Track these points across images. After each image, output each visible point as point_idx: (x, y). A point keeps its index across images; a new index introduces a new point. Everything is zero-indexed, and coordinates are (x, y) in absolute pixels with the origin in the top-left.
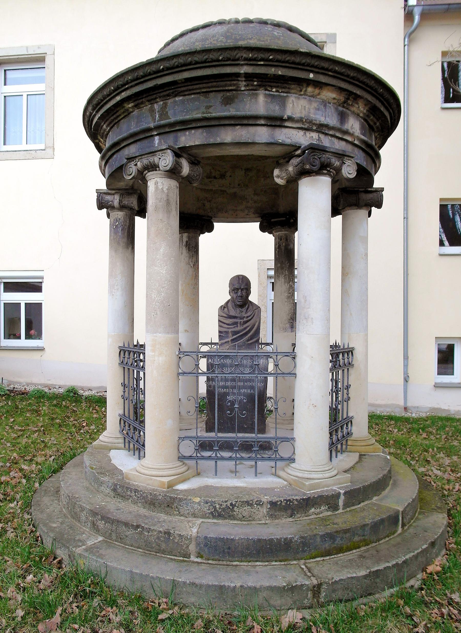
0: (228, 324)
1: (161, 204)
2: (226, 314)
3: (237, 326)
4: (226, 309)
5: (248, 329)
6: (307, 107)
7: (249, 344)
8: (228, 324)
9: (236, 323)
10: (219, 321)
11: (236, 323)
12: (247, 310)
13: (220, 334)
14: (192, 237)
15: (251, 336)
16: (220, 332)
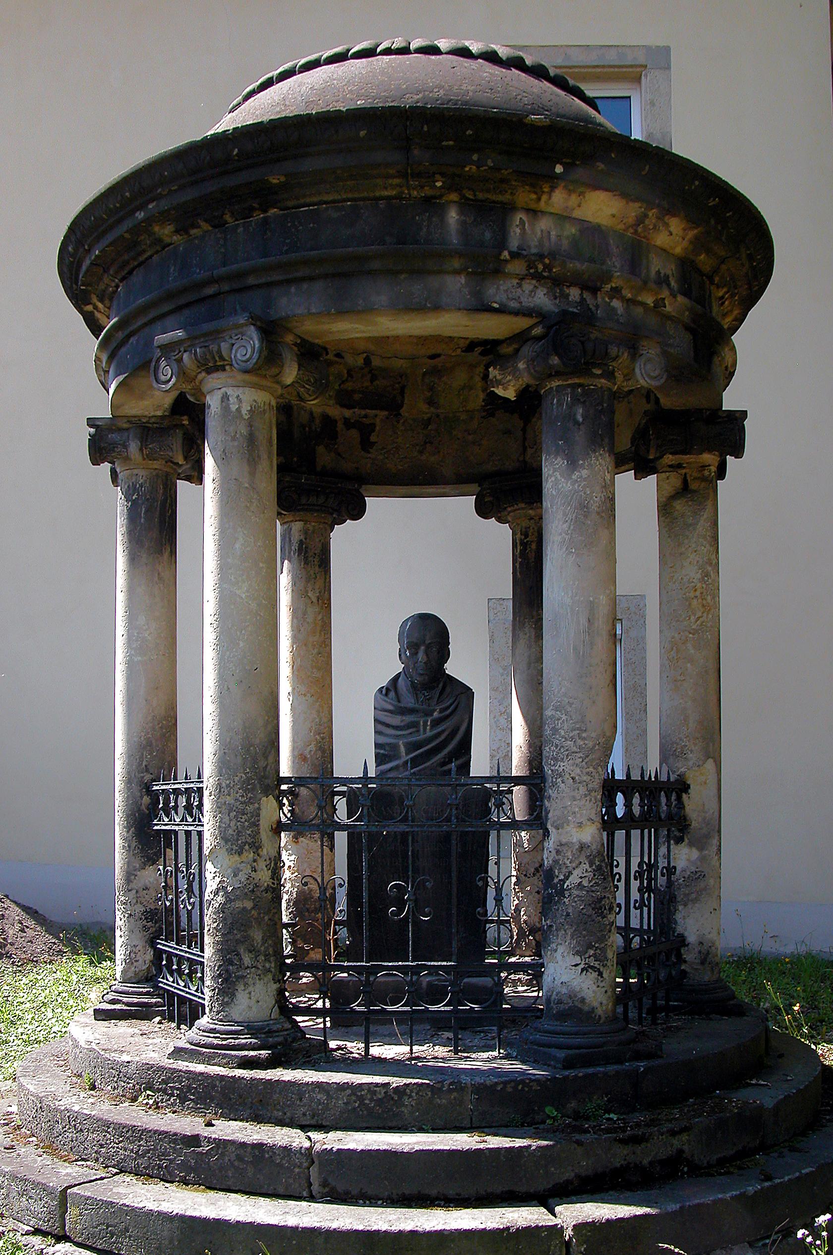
0: (396, 728)
1: (236, 443)
2: (392, 705)
3: (418, 731)
4: (392, 694)
5: (443, 737)
6: (553, 233)
7: (445, 771)
8: (396, 728)
9: (414, 725)
10: (376, 721)
11: (414, 725)
12: (441, 693)
13: (378, 751)
14: (313, 532)
15: (449, 753)
16: (377, 746)
